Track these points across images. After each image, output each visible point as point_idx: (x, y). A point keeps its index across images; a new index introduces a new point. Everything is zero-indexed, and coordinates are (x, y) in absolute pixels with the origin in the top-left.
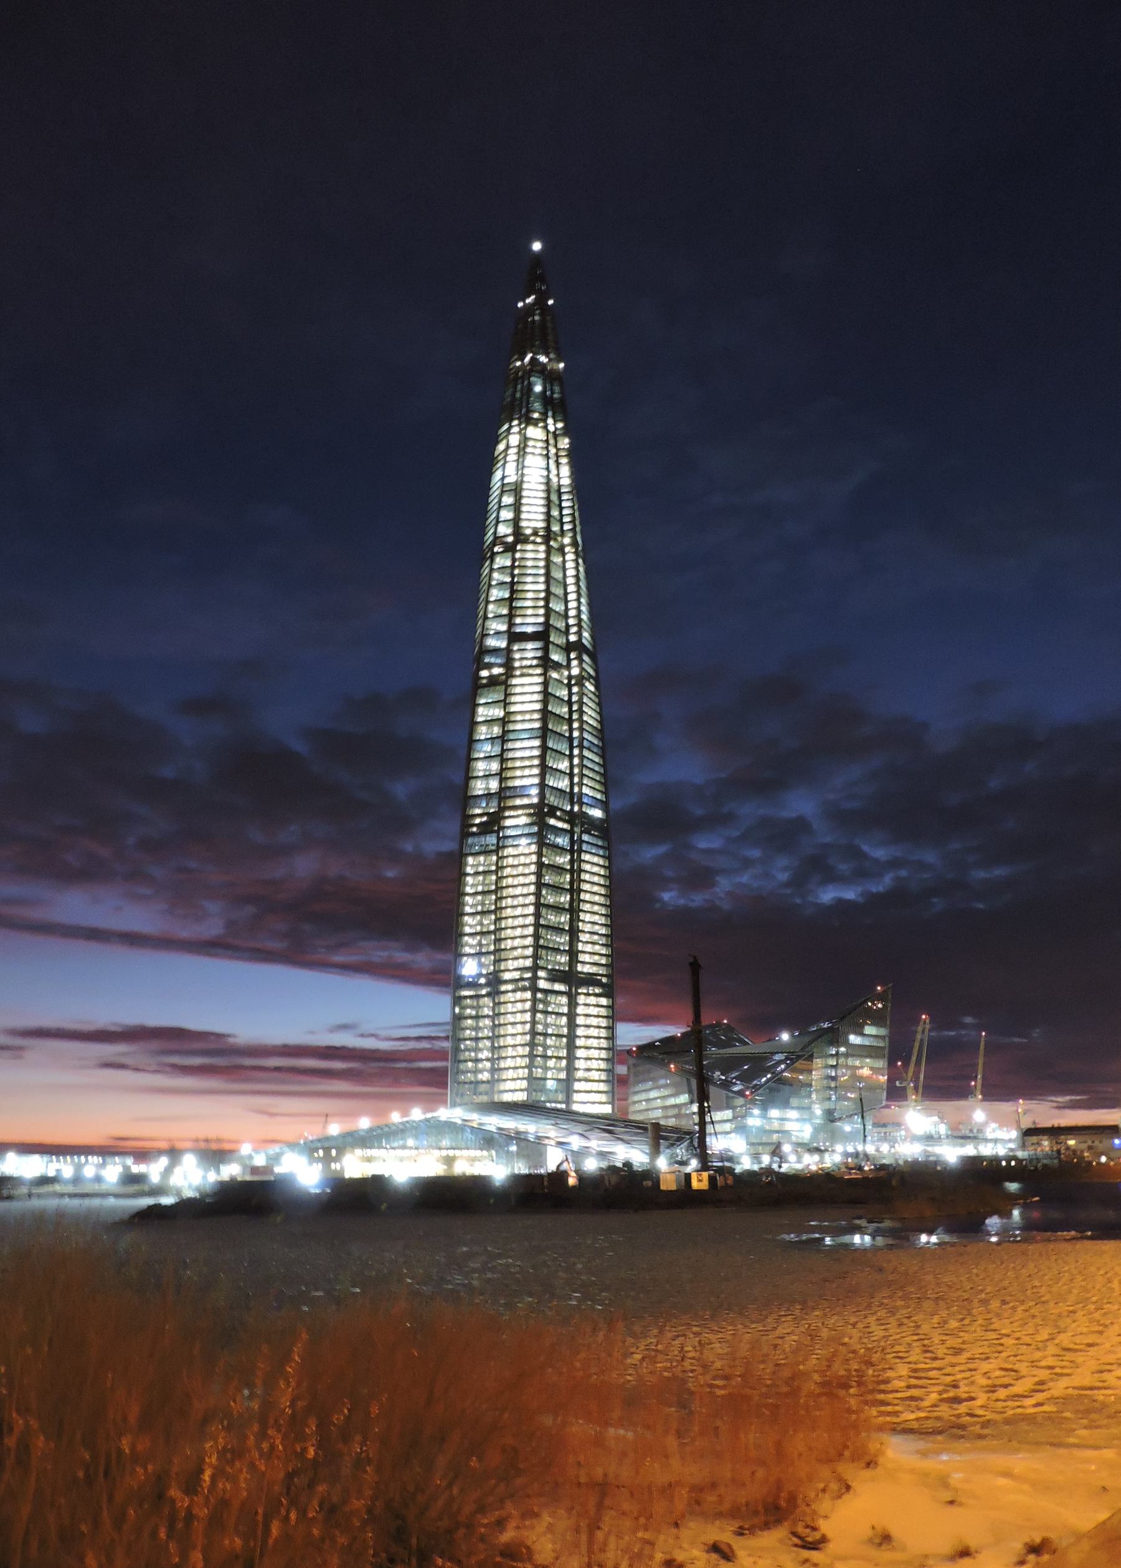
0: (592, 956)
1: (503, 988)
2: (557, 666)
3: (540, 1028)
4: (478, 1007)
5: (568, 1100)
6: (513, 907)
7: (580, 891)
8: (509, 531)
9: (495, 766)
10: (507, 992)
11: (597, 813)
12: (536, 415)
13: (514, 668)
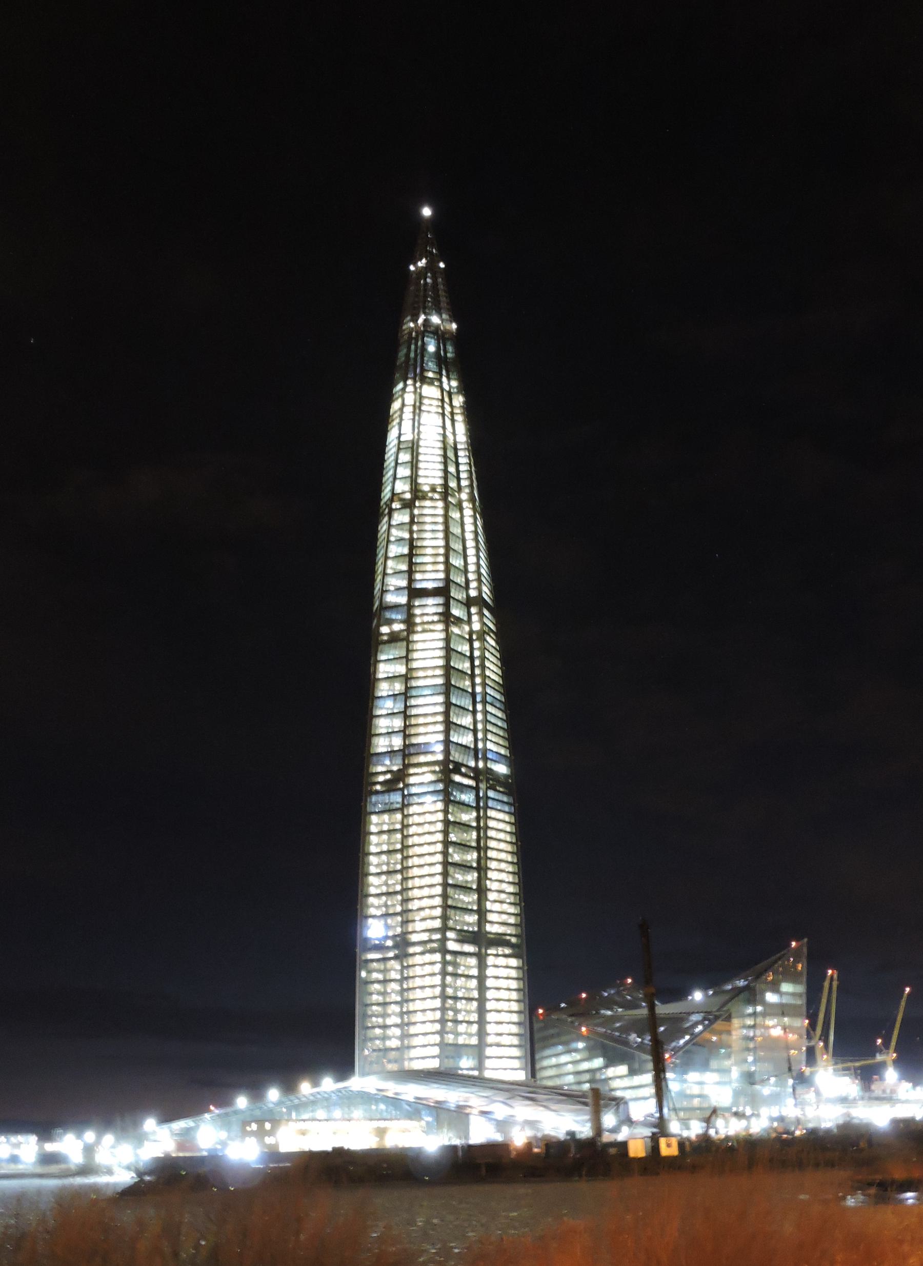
2: (458, 621)
3: (450, 991)
4: (385, 971)
5: (480, 1067)
7: (487, 848)
8: (407, 487)
9: (398, 723)
11: (501, 769)
12: (430, 375)
13: (415, 624)
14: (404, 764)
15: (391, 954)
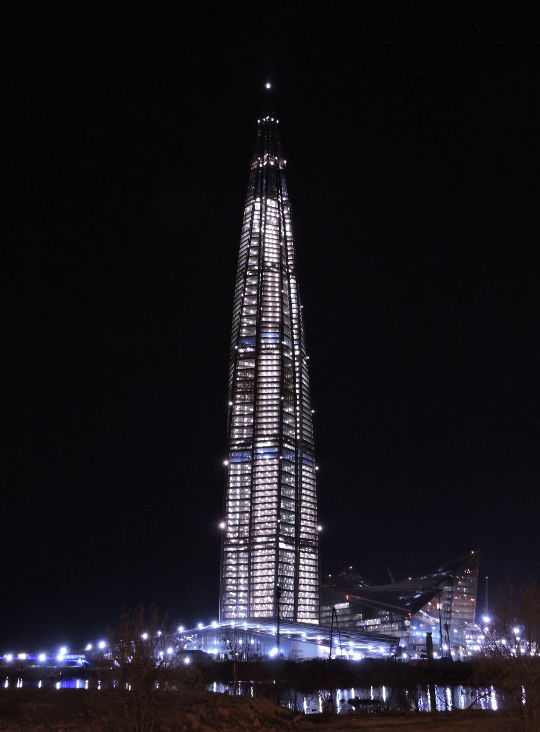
1: (256, 547)
5: (295, 617)
6: (262, 497)
14: (253, 434)
15: (242, 549)
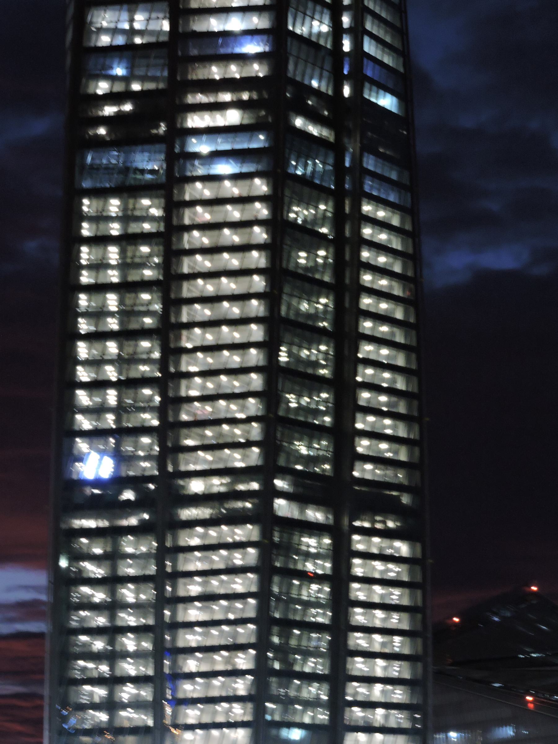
0: (381, 442)
6: (205, 325)
10: (191, 524)
15: (133, 521)
